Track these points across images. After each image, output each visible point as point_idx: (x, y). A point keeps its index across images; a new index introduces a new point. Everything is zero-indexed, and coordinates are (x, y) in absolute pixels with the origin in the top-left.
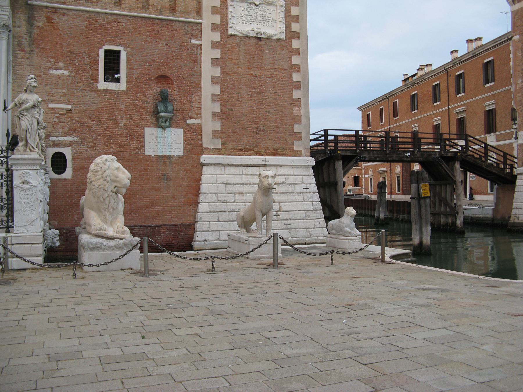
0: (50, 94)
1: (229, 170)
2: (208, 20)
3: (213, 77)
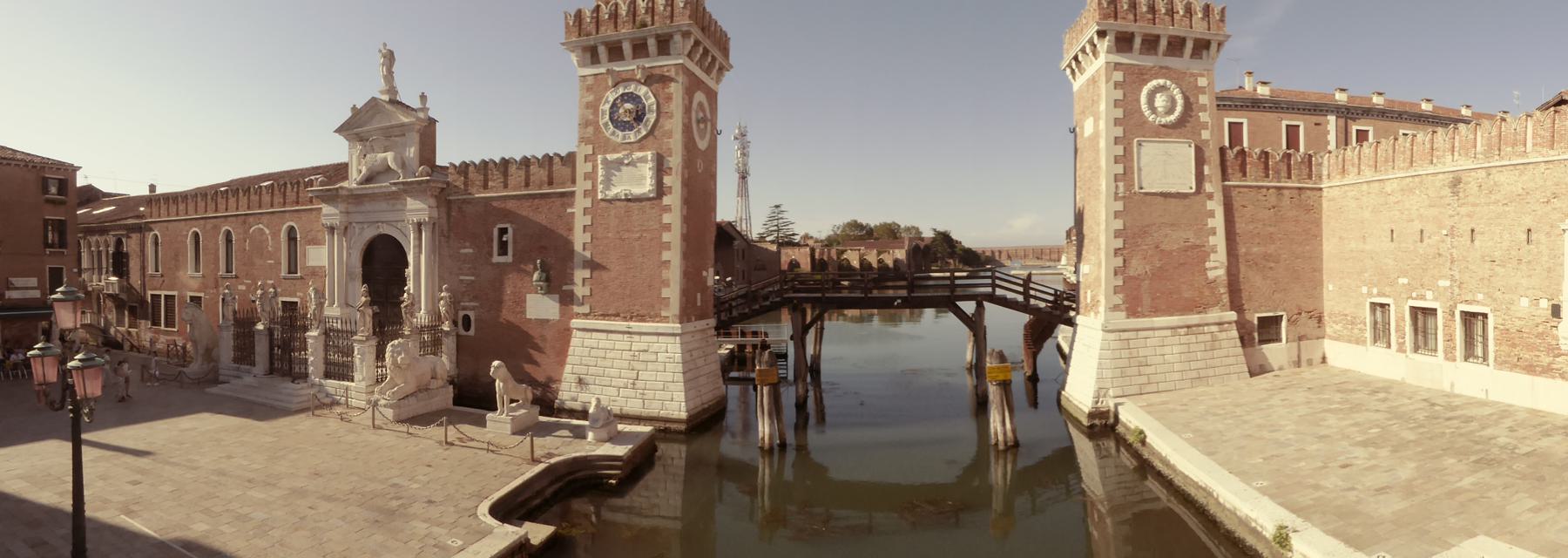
1: (595, 335)
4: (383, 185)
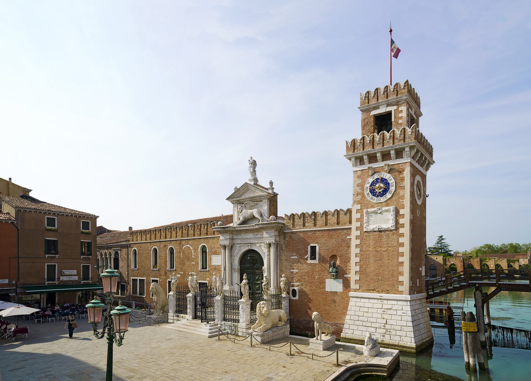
0: (291, 266)
1: (362, 300)
4: (252, 225)
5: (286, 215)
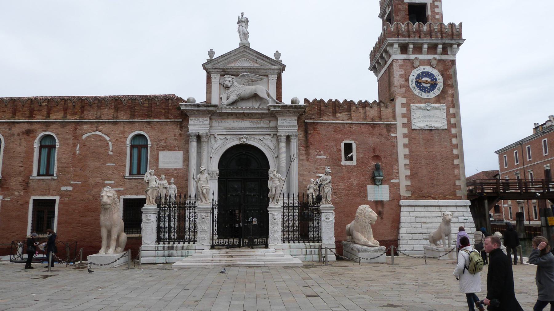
0: (317, 169)
1: (417, 209)
2: (400, 121)
3: (405, 155)
5: (306, 100)
